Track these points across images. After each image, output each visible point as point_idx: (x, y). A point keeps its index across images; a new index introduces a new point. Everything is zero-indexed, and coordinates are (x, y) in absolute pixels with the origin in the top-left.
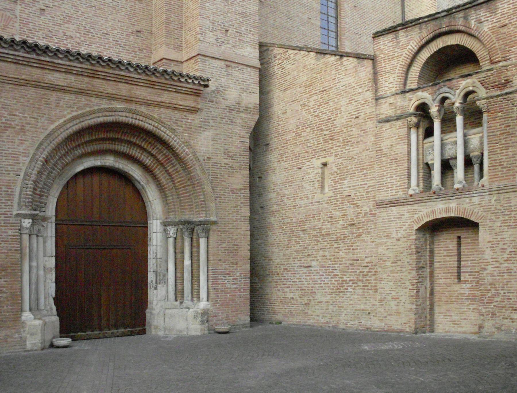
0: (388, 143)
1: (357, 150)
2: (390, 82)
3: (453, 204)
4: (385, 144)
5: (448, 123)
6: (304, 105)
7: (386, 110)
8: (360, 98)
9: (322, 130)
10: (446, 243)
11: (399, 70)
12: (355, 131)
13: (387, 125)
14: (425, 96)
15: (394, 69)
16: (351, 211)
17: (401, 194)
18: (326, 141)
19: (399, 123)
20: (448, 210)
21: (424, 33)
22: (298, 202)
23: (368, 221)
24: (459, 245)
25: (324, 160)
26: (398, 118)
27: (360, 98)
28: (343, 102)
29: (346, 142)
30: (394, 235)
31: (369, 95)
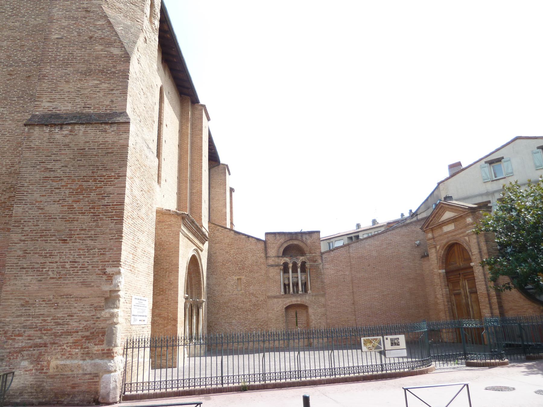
0: (272, 274)
1: (256, 275)
2: (272, 252)
3: (299, 299)
4: (271, 275)
5: (295, 271)
6: (227, 252)
7: (271, 262)
8: (258, 255)
9: (238, 264)
10: (292, 313)
11: (276, 248)
12: (255, 267)
13: (272, 268)
14: (287, 259)
15: (274, 247)
16: (254, 299)
17: (278, 294)
18: (240, 269)
19: (277, 268)
20: (297, 301)
21: (287, 238)
22: (223, 294)
23: (263, 303)
24: (296, 314)
25: (239, 277)
26: (277, 266)
27: (258, 255)
28: (249, 255)
29: (251, 271)
30: (275, 309)
31: (263, 255)
